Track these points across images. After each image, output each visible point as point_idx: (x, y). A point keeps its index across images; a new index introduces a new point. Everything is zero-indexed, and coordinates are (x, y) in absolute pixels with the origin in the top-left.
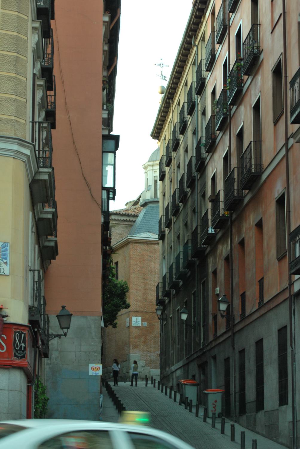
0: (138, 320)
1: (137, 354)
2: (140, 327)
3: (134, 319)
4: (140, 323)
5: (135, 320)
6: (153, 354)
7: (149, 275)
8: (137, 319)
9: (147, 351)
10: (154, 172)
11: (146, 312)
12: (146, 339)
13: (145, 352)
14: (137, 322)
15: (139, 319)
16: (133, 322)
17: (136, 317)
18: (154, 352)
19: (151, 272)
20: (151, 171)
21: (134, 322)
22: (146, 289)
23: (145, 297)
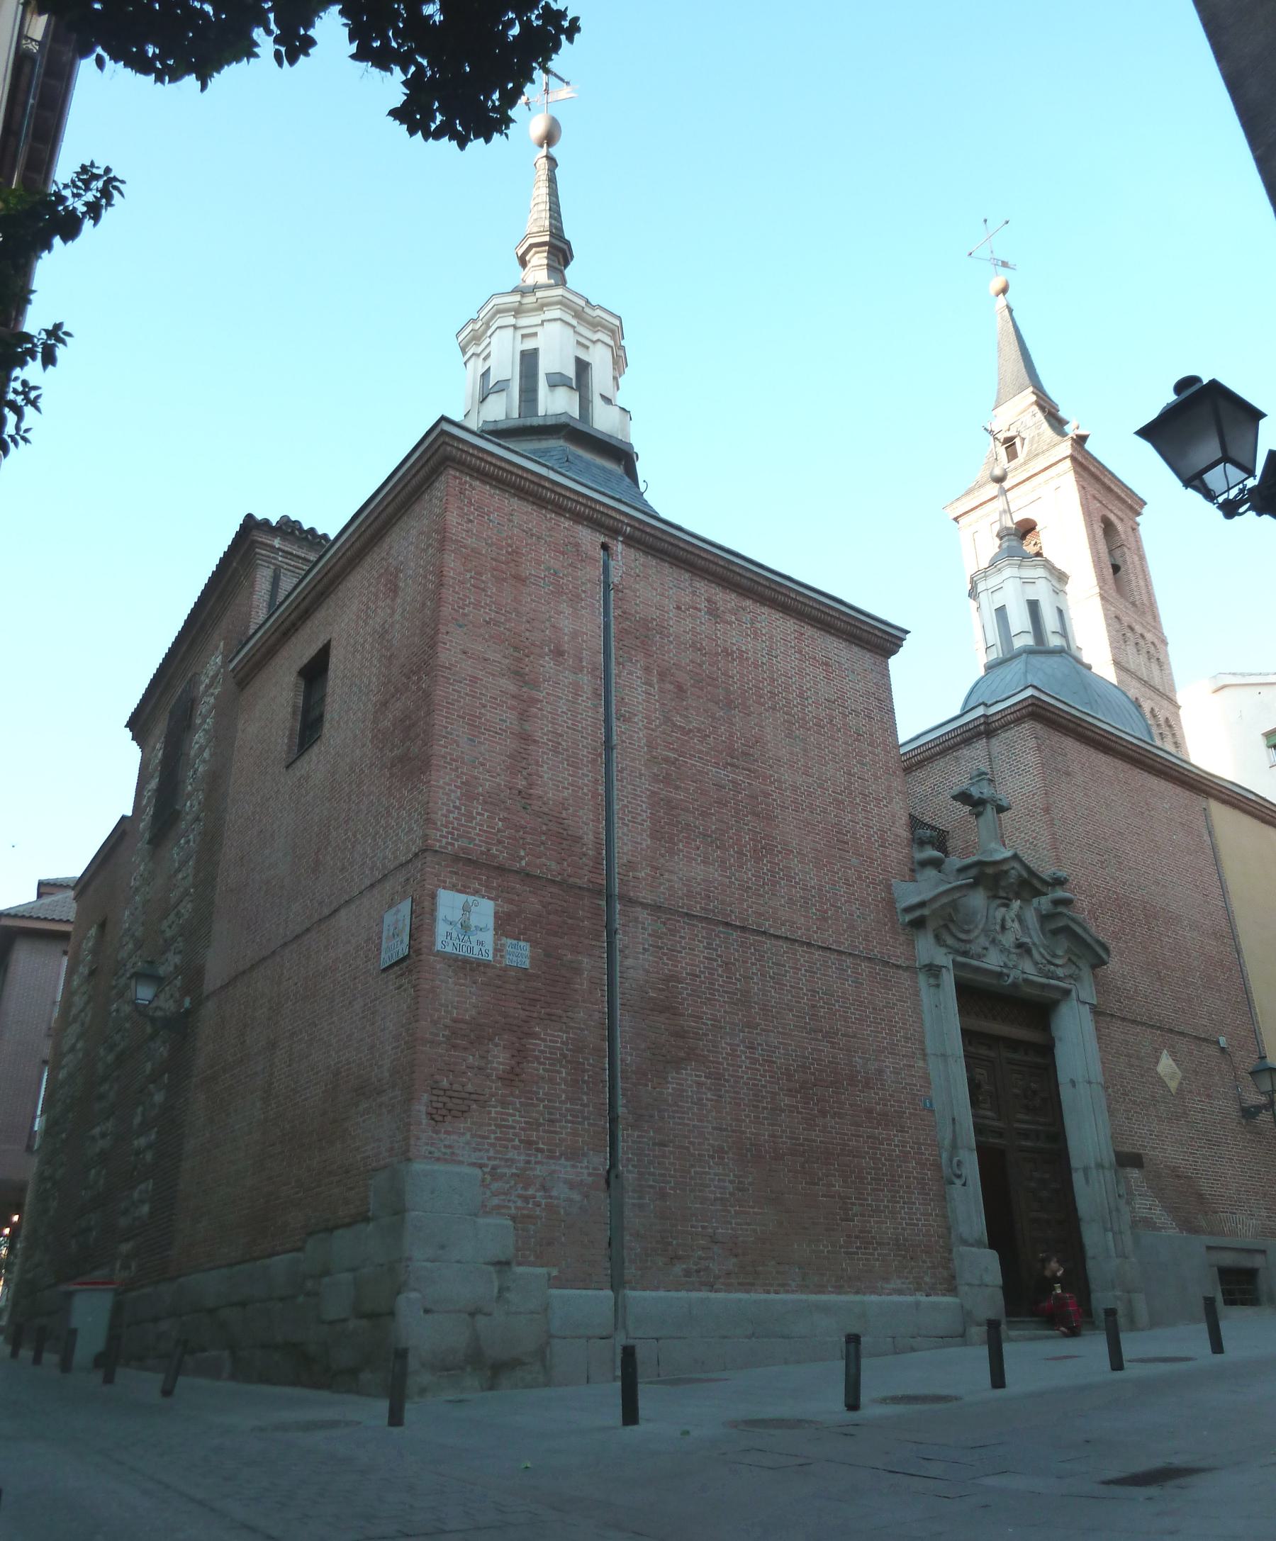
0: (474, 921)
1: (461, 1163)
2: (487, 965)
3: (449, 904)
4: (488, 937)
5: (457, 915)
6: (565, 1170)
7: (548, 664)
8: (466, 909)
9: (529, 1143)
10: (524, 336)
11: (527, 876)
12: (520, 1054)
13: (512, 1154)
14: (465, 927)
15: (484, 911)
16: (442, 929)
17: (461, 898)
18: (574, 1155)
19: (558, 653)
20: (511, 329)
21: (449, 928)
22: (525, 738)
23: (521, 783)
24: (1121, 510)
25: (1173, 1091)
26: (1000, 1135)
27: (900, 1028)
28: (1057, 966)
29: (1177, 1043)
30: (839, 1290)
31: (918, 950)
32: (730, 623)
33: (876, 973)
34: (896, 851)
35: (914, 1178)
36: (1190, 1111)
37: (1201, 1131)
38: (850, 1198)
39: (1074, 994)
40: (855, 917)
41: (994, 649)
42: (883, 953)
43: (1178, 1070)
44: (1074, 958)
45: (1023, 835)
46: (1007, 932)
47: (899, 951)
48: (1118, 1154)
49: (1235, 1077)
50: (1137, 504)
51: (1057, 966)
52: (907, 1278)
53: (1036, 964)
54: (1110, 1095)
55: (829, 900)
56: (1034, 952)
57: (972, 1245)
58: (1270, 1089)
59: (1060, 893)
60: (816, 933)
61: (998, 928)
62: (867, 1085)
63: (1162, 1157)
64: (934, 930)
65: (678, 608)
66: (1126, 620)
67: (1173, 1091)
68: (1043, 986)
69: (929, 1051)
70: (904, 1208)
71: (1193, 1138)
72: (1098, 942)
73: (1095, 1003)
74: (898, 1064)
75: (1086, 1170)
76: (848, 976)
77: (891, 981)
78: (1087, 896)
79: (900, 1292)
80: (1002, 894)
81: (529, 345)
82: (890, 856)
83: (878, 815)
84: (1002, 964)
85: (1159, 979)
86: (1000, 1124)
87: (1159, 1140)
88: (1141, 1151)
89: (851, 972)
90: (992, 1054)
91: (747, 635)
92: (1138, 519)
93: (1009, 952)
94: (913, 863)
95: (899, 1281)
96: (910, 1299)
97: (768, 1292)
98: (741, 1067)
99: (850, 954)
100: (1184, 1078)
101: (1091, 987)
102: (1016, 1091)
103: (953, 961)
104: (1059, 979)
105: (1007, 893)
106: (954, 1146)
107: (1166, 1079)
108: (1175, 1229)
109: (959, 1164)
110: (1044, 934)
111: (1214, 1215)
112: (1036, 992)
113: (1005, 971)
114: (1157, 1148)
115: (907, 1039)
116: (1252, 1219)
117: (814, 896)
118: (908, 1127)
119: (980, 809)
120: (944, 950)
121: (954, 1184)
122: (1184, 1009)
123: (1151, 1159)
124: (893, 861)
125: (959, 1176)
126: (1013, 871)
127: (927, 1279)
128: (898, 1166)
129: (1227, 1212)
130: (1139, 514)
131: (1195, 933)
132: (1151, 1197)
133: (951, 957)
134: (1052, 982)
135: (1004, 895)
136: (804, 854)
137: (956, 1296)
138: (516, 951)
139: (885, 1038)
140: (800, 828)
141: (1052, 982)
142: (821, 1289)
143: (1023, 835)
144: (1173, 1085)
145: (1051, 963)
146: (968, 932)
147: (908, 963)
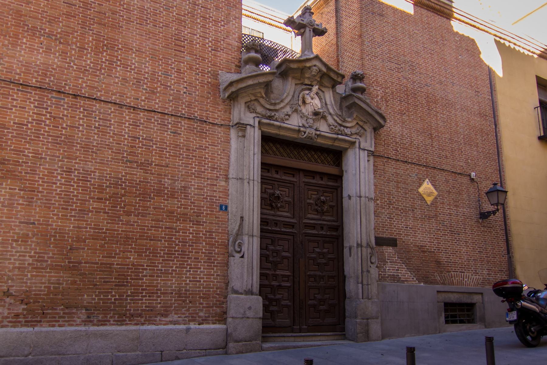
25: (429, 203)
26: (292, 226)
27: (209, 162)
28: (347, 127)
29: (438, 175)
30: (121, 322)
31: (233, 115)
33: (194, 128)
34: (227, 53)
35: (202, 253)
36: (440, 214)
37: (447, 226)
38: (143, 266)
39: (357, 144)
40: (182, 93)
42: (202, 116)
43: (434, 191)
44: (360, 123)
46: (307, 105)
47: (216, 115)
48: (377, 238)
49: (479, 195)
51: (347, 127)
52: (184, 314)
53: (329, 126)
54: (378, 204)
55: (160, 81)
56: (329, 118)
57: (241, 294)
58: (496, 202)
59: (359, 84)
60: (144, 101)
61: (300, 102)
62: (172, 195)
63: (413, 240)
64: (245, 103)
67: (429, 203)
68: (335, 139)
69: (230, 176)
70: (190, 271)
71: (440, 230)
72: (377, 113)
73: (372, 149)
74: (203, 184)
75: (350, 248)
76: (168, 129)
77: (206, 133)
78: (382, 88)
80: (307, 82)
82: (220, 57)
83: (215, 31)
84: (301, 125)
85: (431, 138)
87: (413, 231)
88: (397, 237)
89: (171, 126)
90: (294, 179)
93: (308, 118)
94: (240, 62)
95: (176, 316)
97: (54, 326)
98: (56, 184)
99: (172, 115)
100: (439, 195)
101: (371, 140)
102: (311, 201)
103: (259, 122)
104: (346, 135)
105: (312, 82)
106: (239, 233)
107: (425, 196)
108: (415, 281)
109: (240, 245)
110: (341, 108)
111: (447, 273)
112: (329, 143)
113: (302, 129)
114: (410, 235)
115: (213, 168)
116: (476, 275)
117: (146, 78)
118: (203, 222)
119: (302, 30)
120: (254, 115)
121: (234, 257)
122: (447, 156)
123: (404, 242)
124: (222, 60)
125: (239, 252)
126: (314, 68)
128: (189, 246)
129: (458, 272)
132: (399, 263)
133: (257, 120)
134: (340, 137)
135: (310, 83)
136: (142, 52)
137: (225, 324)
139: (195, 168)
140: (142, 35)
141: (340, 137)
142: (103, 323)
144: (429, 200)
145: (341, 125)
146: (275, 104)
147: (223, 123)
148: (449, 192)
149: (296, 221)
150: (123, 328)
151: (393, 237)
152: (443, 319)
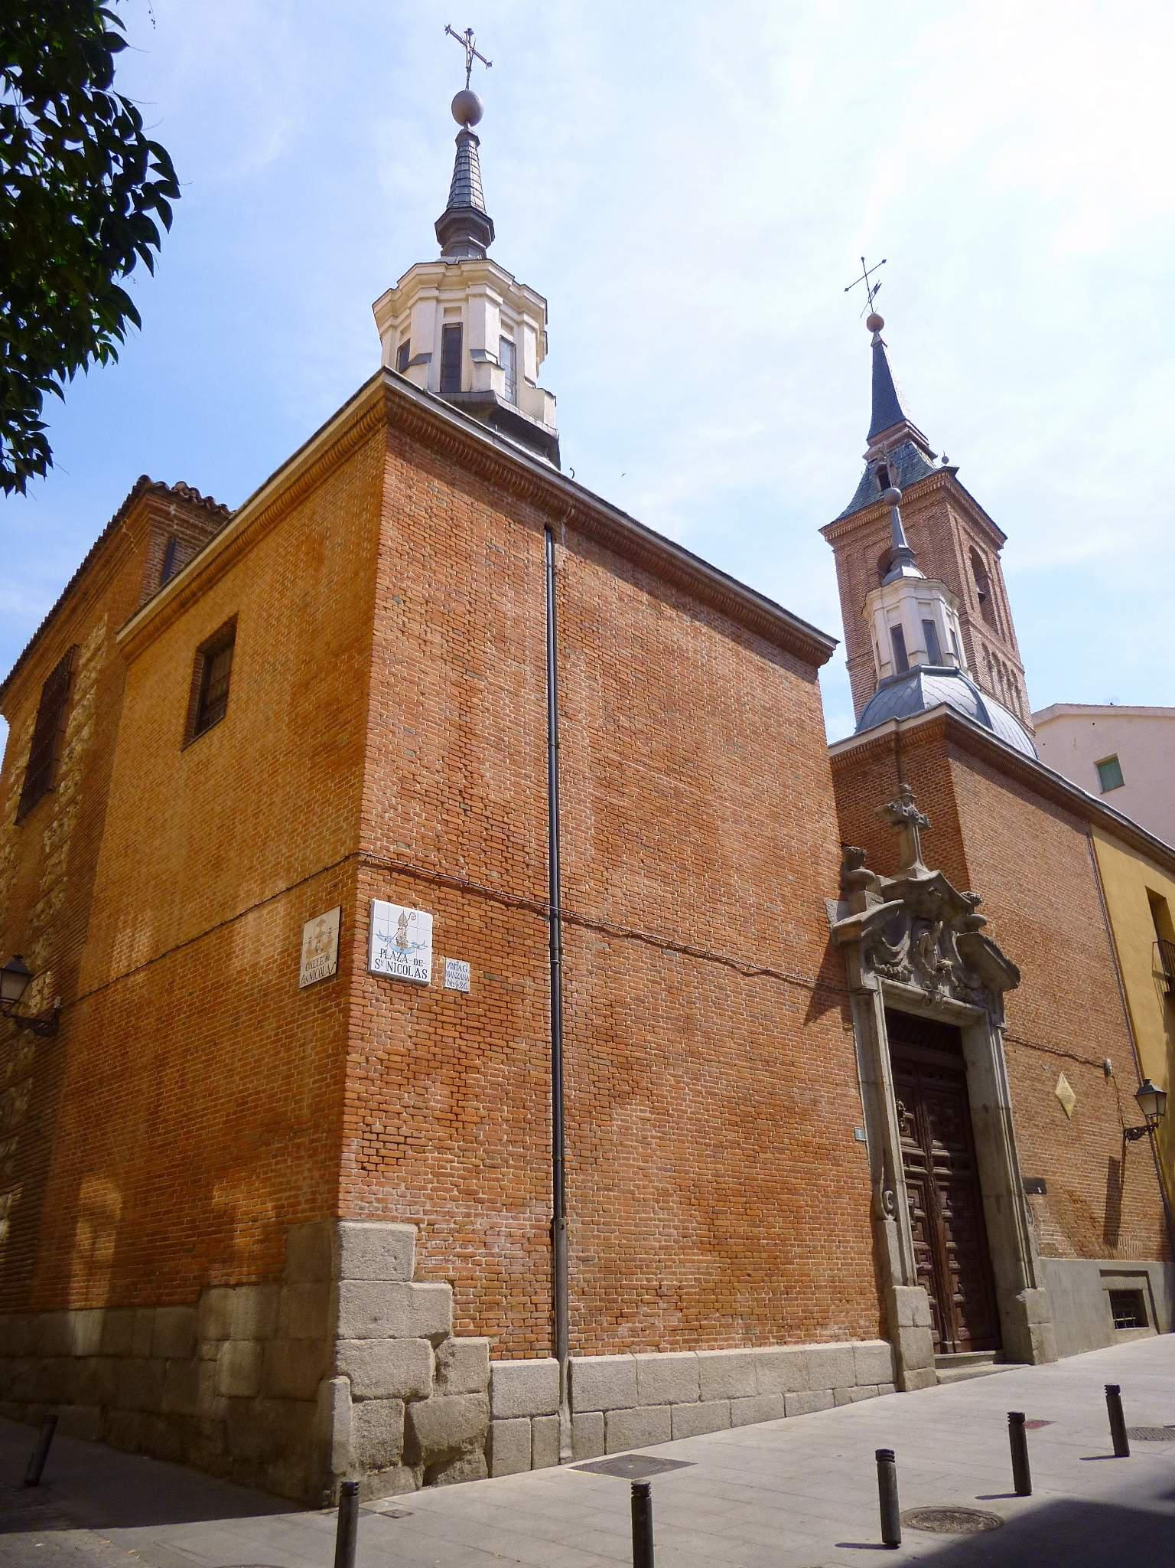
0: (410, 938)
1: (394, 1220)
2: (424, 985)
3: (386, 916)
4: (427, 956)
5: (393, 931)
6: (505, 1221)
8: (403, 923)
9: (469, 1193)
11: (466, 889)
12: (460, 1090)
13: (450, 1206)
14: (402, 944)
15: (422, 924)
16: (377, 945)
17: (397, 910)
18: (515, 1205)
19: (501, 639)
20: (434, 302)
21: (383, 945)
23: (460, 780)
24: (985, 543)
32: (671, 619)
41: (889, 666)
43: (1073, 1094)
45: (932, 854)
50: (999, 538)
52: (843, 1322)
62: (804, 1115)
65: (621, 599)
66: (991, 648)
79: (837, 1338)
81: (452, 319)
86: (920, 1152)
91: (687, 633)
92: (1000, 552)
96: (846, 1345)
100: (1078, 1101)
103: (883, 983)
114: (1056, 1172)
127: (862, 1322)
130: (999, 547)
131: (1083, 957)
138: (455, 972)
142: (762, 1341)
143: (932, 854)
148: (1087, 1095)
149: (922, 1153)
150: (786, 1349)
151: (1040, 1176)
152: (1111, 1321)
